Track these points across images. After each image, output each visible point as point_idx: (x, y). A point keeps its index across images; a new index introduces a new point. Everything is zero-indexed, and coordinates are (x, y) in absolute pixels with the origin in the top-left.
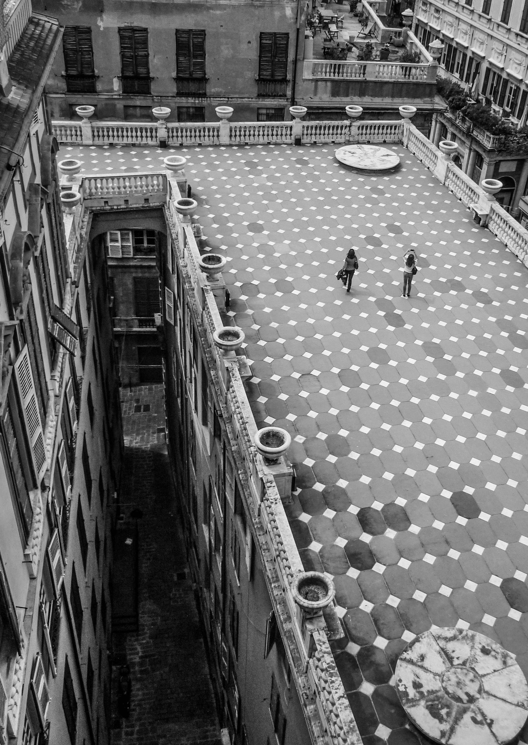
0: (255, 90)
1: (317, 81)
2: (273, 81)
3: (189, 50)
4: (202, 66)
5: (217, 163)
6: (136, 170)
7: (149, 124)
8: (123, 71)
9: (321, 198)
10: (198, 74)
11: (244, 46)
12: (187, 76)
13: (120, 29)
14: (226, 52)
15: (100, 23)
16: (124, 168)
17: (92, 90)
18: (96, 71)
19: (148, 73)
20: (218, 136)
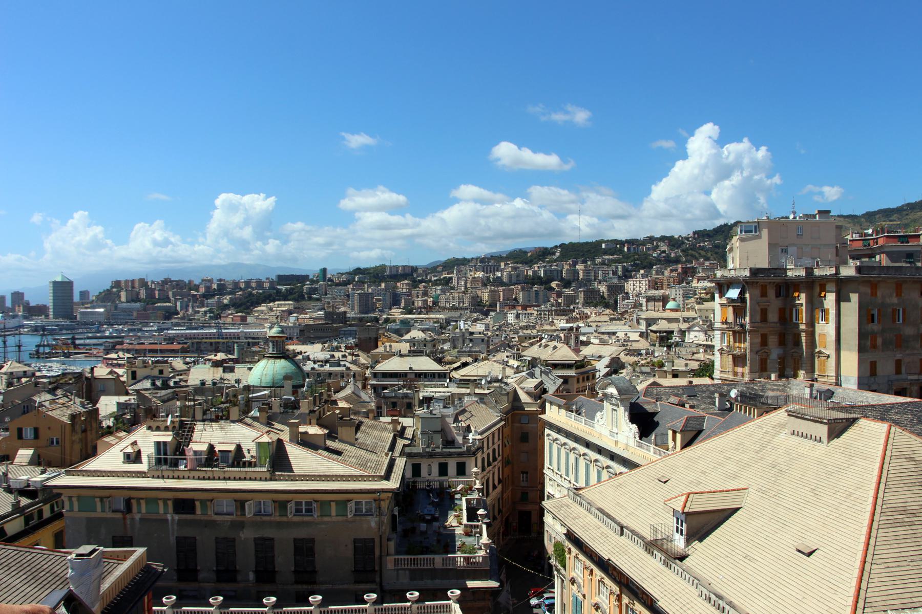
1: (398, 570)
13: (255, 539)
15: (242, 535)
17: (234, 580)
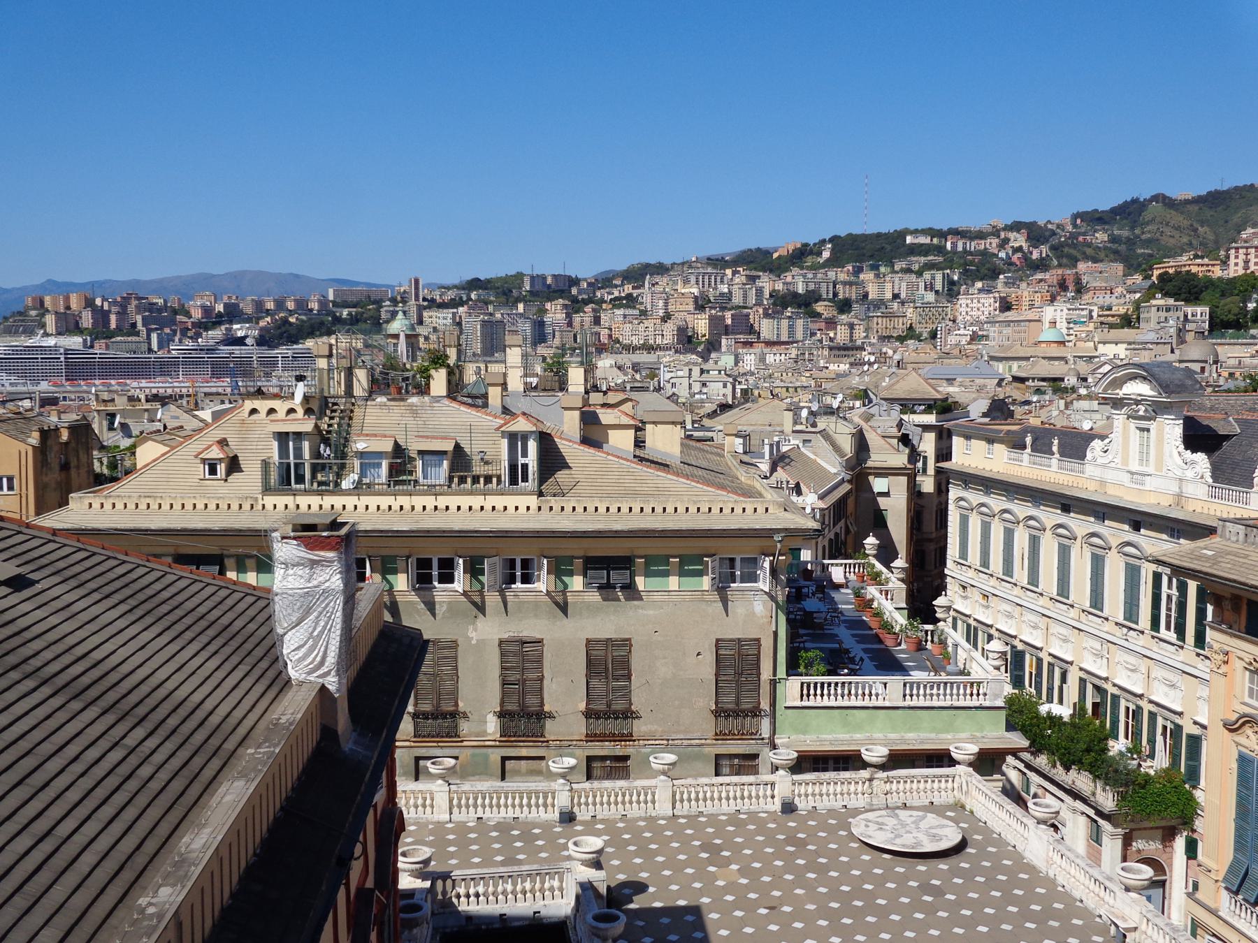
0: (708, 726)
2: (737, 713)
3: (606, 669)
4: (627, 694)
5: (653, 846)
6: (520, 862)
7: (542, 785)
8: (502, 703)
9: (835, 905)
10: (619, 705)
11: (692, 659)
12: (603, 707)
13: (501, 642)
14: (664, 670)
16: (499, 858)
18: (461, 704)
19: (542, 704)
20: (653, 802)
